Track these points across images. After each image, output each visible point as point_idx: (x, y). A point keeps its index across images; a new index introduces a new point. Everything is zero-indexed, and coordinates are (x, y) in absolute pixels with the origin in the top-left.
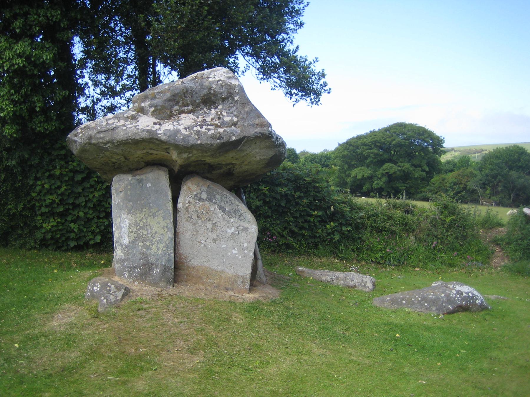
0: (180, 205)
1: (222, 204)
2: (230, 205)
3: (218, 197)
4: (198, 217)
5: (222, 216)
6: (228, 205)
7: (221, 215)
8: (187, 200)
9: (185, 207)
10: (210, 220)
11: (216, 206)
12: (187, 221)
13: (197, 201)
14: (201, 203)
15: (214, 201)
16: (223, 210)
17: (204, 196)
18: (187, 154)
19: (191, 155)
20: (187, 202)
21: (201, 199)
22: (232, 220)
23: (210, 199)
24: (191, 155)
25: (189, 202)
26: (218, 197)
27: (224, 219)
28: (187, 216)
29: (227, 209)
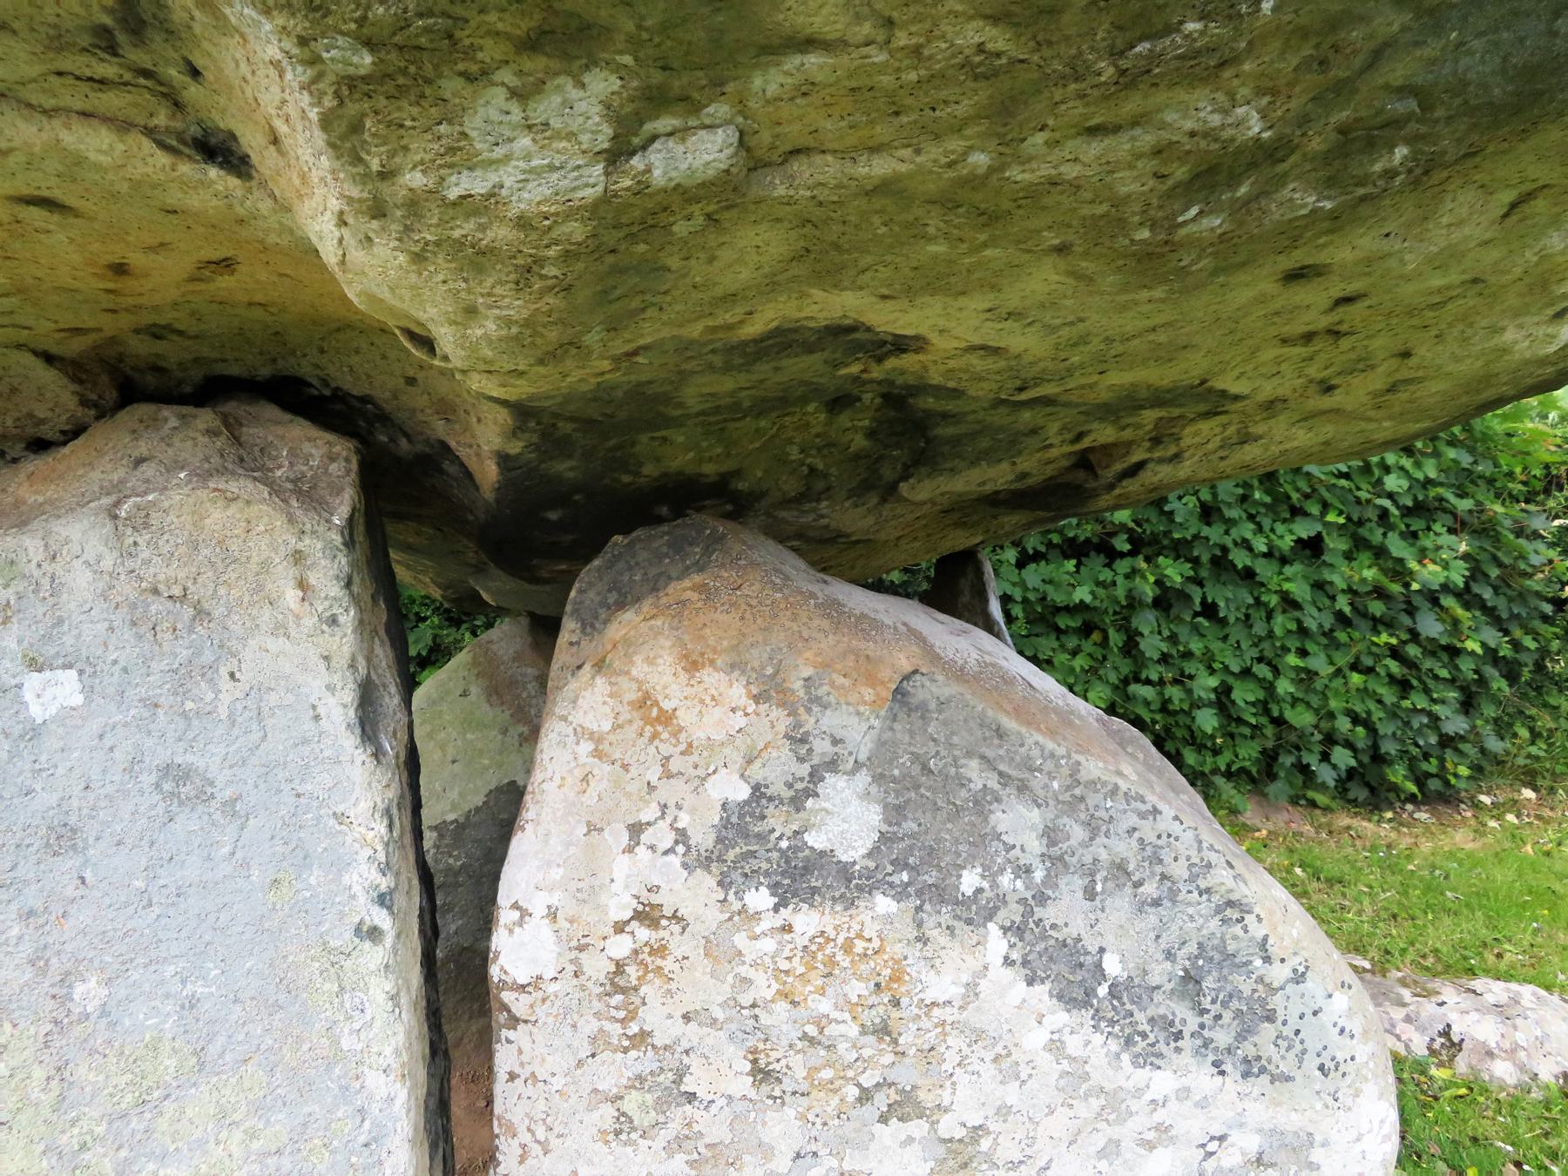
0: (518, 952)
1: (1067, 912)
2: (1141, 907)
3: (1019, 823)
4: (762, 1074)
5: (1055, 1046)
6: (1120, 905)
7: (1036, 1039)
8: (626, 877)
9: (597, 967)
10: (904, 1107)
11: (997, 943)
12: (623, 1127)
13: (760, 899)
14: (807, 921)
15: (970, 881)
16: (1071, 975)
17: (847, 821)
18: (585, 102)
19: (696, 153)
20: (621, 908)
21: (802, 877)
22: (1162, 1082)
23: (920, 863)
24: (696, 153)
25: (647, 915)
26: (1019, 823)
27: (1076, 1077)
28: (612, 1071)
29: (1112, 966)
